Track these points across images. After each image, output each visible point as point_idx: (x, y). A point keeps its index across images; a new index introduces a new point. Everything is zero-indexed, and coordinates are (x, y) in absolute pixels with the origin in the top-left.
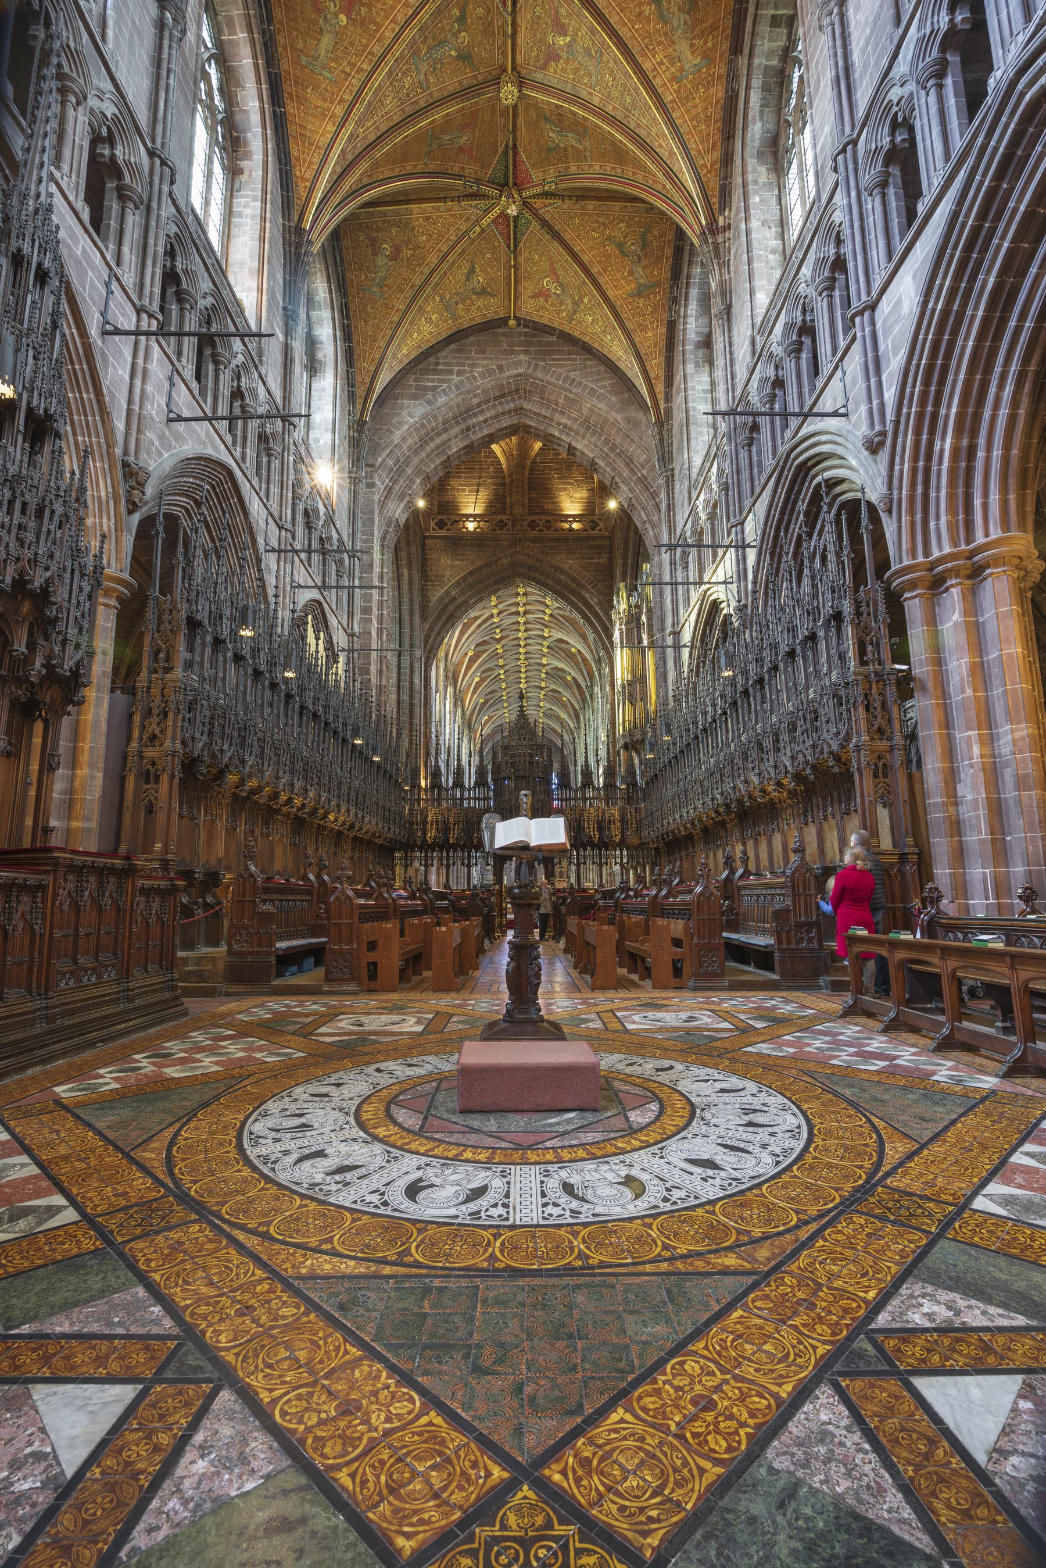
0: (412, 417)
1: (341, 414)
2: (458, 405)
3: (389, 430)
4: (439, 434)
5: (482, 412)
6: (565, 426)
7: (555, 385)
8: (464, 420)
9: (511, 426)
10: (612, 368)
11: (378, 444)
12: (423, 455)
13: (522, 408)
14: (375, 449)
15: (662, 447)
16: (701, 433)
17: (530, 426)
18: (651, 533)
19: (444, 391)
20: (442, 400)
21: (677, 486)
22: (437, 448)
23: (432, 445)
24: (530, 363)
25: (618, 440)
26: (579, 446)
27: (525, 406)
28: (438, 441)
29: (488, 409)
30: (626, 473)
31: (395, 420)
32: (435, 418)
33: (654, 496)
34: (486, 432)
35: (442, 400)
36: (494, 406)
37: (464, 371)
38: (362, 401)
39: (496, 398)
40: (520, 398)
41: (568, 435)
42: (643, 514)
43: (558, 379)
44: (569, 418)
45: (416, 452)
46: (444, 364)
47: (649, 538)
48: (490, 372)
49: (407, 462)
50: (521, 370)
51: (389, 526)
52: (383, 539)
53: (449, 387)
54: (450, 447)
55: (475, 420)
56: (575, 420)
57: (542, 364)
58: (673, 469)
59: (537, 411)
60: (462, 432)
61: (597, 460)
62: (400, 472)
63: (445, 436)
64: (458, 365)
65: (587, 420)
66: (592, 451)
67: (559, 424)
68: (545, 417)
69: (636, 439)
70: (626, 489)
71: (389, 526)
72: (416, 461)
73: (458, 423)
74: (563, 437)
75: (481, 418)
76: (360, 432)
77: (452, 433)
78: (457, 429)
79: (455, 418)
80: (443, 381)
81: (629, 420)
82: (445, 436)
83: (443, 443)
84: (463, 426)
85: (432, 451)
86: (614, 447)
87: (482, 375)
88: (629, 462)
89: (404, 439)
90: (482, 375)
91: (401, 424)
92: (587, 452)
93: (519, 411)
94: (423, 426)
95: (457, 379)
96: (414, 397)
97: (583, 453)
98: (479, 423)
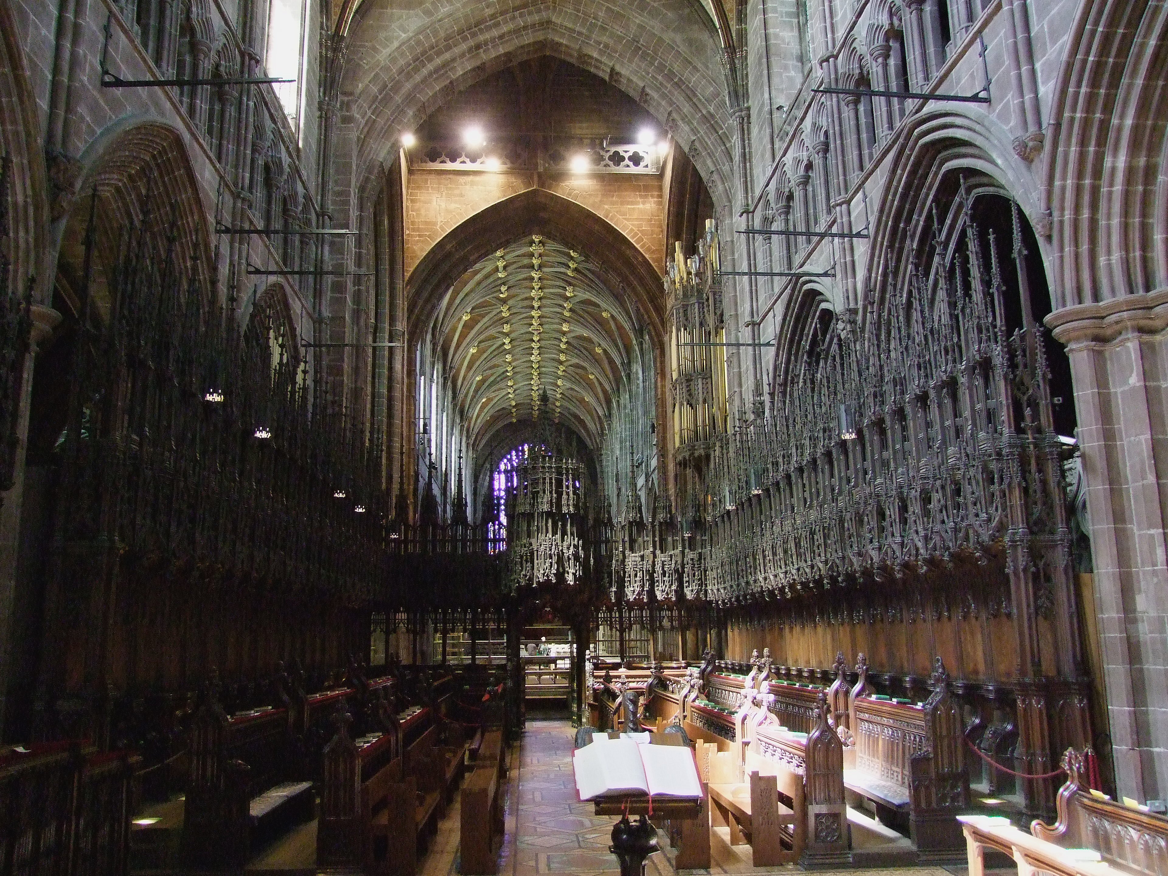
0: (404, 31)
1: (311, 30)
2: (466, 16)
3: (374, 49)
4: (439, 54)
5: (497, 25)
6: (606, 46)
8: (474, 35)
9: (535, 43)
12: (418, 78)
13: (549, 22)
16: (786, 68)
17: (560, 44)
18: (720, 187)
21: (755, 131)
22: (437, 70)
23: (430, 67)
25: (676, 67)
26: (624, 72)
27: (554, 19)
28: (438, 61)
29: (506, 22)
30: (687, 109)
31: (382, 35)
32: (435, 33)
33: (723, 139)
34: (501, 50)
36: (513, 18)
38: (338, 11)
39: (515, 9)
40: (547, 8)
41: (610, 56)
42: (709, 162)
44: (612, 35)
45: (409, 76)
47: (717, 192)
49: (397, 87)
52: (362, 189)
54: (453, 69)
55: (487, 36)
56: (620, 39)
58: (748, 109)
59: (570, 25)
60: (470, 50)
61: (648, 90)
62: (386, 100)
63: (447, 56)
65: (635, 40)
66: (642, 78)
67: (599, 43)
68: (580, 33)
69: (699, 66)
70: (687, 128)
72: (408, 86)
73: (465, 39)
74: (604, 59)
75: (495, 33)
76: (336, 50)
77: (457, 50)
78: (464, 47)
79: (461, 32)
81: (690, 42)
82: (447, 56)
83: (445, 65)
84: (471, 43)
85: (430, 74)
86: (670, 76)
88: (690, 95)
89: (393, 60)
92: (635, 79)
93: (546, 25)
94: (419, 43)
97: (629, 80)
98: (493, 40)
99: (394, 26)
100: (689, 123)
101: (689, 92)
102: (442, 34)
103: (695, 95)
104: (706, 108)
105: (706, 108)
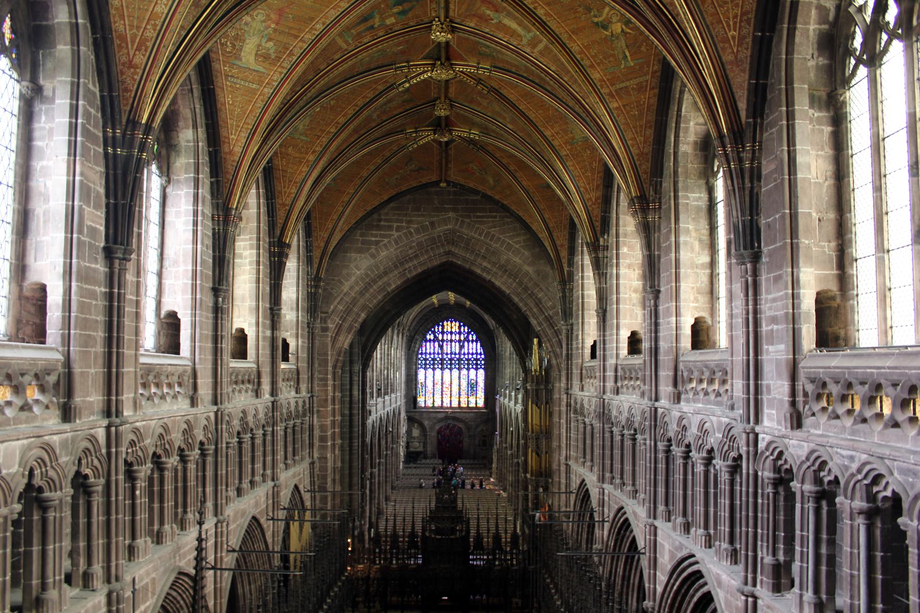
0: (359, 270)
2: (397, 257)
7: (479, 240)
10: (527, 227)
11: (331, 293)
14: (328, 298)
15: (565, 303)
19: (385, 245)
20: (384, 254)
24: (457, 220)
31: (345, 272)
32: (377, 267)
35: (384, 254)
37: (402, 228)
43: (480, 235)
46: (386, 220)
48: (424, 229)
50: (449, 227)
51: (339, 356)
53: (389, 242)
57: (467, 220)
64: (397, 221)
71: (339, 356)
80: (384, 236)
86: (526, 289)
87: (417, 231)
88: (538, 302)
89: (351, 288)
90: (417, 231)
91: (349, 275)
95: (395, 234)
96: (360, 251)
99: (352, 266)
100: (537, 318)
101: (537, 301)
102: (382, 268)
103: (541, 303)
104: (547, 312)
105: (547, 312)
